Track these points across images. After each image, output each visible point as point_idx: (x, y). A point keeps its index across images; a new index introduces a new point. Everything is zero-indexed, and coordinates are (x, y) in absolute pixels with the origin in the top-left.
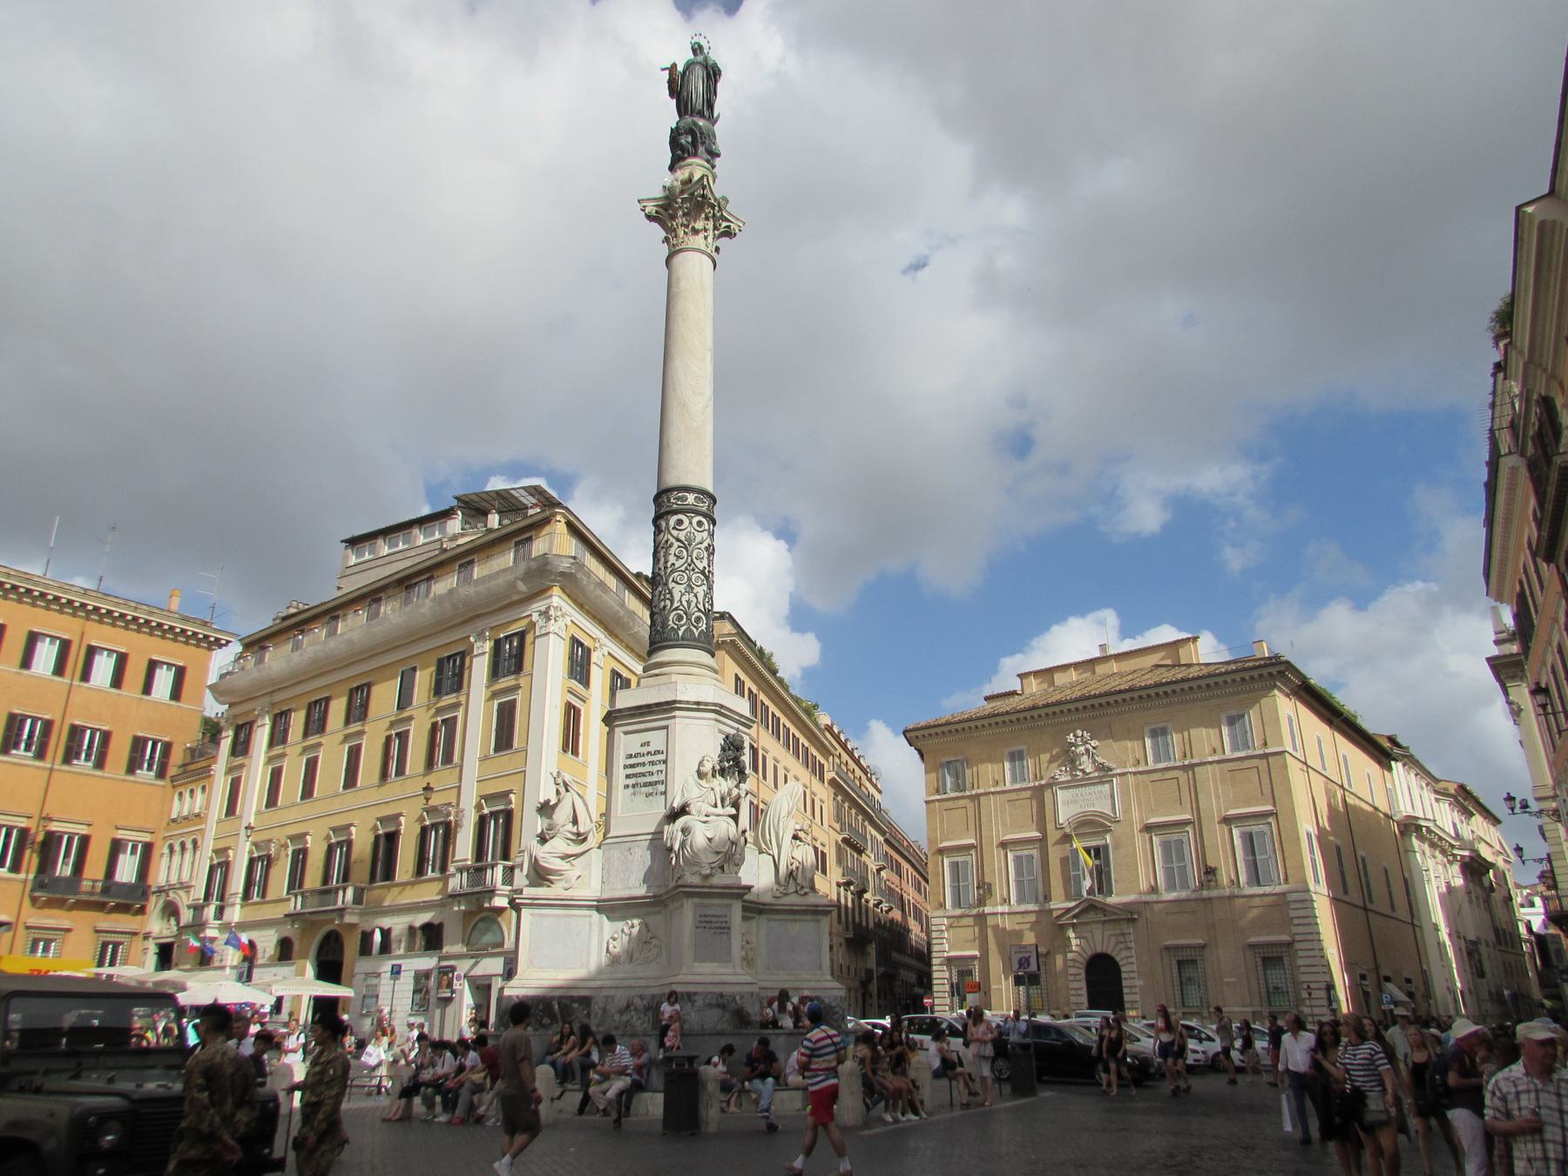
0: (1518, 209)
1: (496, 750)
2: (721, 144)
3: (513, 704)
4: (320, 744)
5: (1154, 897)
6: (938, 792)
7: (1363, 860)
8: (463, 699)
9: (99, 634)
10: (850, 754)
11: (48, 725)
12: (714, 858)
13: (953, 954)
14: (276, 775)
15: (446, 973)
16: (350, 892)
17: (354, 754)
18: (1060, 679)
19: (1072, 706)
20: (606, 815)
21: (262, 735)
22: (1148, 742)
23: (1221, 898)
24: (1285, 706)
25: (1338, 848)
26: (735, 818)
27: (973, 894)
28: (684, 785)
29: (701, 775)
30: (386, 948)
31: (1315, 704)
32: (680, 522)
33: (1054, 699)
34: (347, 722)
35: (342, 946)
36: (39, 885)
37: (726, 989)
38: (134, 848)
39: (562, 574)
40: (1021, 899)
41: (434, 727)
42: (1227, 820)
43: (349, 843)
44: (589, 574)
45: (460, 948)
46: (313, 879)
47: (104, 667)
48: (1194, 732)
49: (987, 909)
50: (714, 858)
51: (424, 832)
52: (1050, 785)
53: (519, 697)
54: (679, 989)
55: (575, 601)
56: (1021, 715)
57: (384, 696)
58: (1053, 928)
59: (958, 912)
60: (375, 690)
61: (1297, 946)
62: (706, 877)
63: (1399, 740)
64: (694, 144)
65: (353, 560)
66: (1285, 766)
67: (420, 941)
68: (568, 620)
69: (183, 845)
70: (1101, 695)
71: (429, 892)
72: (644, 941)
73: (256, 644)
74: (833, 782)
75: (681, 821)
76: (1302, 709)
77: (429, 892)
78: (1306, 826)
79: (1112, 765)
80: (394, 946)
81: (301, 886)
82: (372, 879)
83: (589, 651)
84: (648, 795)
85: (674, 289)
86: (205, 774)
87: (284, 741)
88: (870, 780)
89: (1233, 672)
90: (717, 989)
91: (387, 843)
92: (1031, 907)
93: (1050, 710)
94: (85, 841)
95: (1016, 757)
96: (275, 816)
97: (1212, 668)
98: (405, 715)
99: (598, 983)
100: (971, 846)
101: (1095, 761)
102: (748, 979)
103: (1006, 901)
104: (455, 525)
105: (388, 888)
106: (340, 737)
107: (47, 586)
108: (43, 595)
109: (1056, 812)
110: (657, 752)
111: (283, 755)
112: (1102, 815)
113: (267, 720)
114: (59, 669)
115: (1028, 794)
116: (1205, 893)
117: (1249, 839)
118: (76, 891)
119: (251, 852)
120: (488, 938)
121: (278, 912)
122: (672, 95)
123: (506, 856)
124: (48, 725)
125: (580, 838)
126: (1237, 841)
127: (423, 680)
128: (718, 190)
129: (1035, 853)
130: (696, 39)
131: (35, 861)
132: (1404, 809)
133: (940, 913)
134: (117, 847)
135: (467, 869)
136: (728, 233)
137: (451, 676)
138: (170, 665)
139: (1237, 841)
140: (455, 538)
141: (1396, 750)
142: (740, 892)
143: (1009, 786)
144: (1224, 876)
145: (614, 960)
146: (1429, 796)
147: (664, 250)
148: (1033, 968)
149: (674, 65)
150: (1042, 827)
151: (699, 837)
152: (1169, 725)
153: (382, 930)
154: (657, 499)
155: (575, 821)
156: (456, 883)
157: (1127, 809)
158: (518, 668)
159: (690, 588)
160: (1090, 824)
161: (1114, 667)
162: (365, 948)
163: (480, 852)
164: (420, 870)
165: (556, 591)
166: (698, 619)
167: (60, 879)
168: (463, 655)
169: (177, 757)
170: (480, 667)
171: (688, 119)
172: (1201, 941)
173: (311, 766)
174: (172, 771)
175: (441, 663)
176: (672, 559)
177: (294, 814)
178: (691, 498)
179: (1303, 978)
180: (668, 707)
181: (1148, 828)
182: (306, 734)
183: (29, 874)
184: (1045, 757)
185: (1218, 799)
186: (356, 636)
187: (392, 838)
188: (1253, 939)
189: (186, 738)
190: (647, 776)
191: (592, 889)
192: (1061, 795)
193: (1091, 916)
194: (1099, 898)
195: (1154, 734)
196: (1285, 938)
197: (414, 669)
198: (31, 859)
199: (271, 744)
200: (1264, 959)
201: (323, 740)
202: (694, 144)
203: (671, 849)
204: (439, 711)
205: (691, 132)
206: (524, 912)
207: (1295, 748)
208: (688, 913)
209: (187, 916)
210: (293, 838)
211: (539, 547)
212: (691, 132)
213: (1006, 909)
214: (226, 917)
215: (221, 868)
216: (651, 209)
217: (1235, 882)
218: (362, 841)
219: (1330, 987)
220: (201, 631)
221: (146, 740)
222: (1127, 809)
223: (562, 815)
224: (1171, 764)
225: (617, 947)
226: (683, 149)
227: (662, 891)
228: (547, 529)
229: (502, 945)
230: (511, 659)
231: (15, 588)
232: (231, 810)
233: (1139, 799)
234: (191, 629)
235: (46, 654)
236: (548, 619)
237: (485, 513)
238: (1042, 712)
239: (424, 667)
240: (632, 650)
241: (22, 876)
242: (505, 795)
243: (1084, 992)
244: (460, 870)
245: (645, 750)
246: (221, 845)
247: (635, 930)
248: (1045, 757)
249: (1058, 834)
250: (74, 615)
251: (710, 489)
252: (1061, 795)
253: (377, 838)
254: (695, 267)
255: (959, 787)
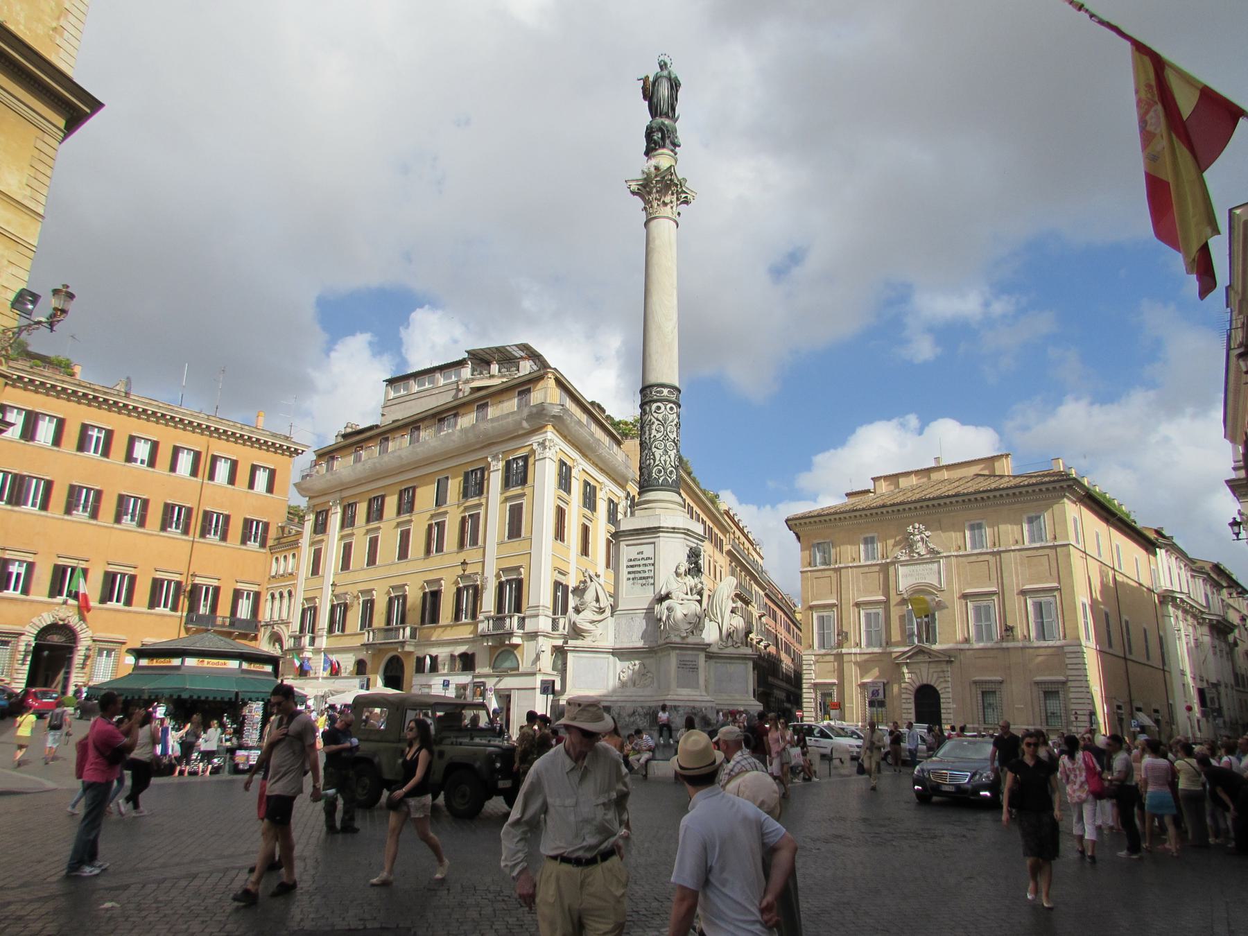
0: (1230, 211)
1: (509, 538)
2: (681, 136)
3: (520, 506)
4: (379, 528)
5: (966, 646)
6: (810, 565)
7: (1127, 622)
8: (483, 501)
9: (220, 447)
10: (741, 530)
11: (190, 510)
12: (688, 626)
13: (818, 681)
14: (347, 549)
15: (480, 688)
16: (408, 630)
17: (405, 536)
18: (903, 482)
19: (912, 506)
20: (615, 596)
21: (335, 520)
22: (968, 533)
23: (1015, 648)
24: (1072, 510)
25: (1107, 615)
26: (700, 602)
27: (834, 639)
28: (666, 579)
29: (678, 574)
30: (434, 668)
31: (1097, 508)
32: (659, 408)
33: (898, 500)
34: (399, 513)
35: (402, 666)
36: (189, 620)
37: (697, 705)
38: (248, 595)
39: (554, 417)
40: (869, 644)
41: (464, 520)
42: (1023, 593)
43: (405, 597)
44: (571, 415)
45: (487, 670)
46: (379, 620)
47: (223, 469)
48: (1002, 527)
49: (844, 651)
50: (688, 626)
51: (459, 592)
52: (893, 563)
53: (525, 501)
54: (668, 703)
55: (561, 434)
56: (874, 511)
57: (425, 496)
58: (894, 667)
59: (823, 651)
60: (418, 491)
61: (1070, 684)
62: (683, 638)
63: (1165, 533)
64: (663, 138)
65: (392, 395)
66: (1069, 555)
67: (458, 664)
68: (557, 448)
69: (281, 595)
70: (934, 499)
71: (464, 632)
72: (643, 673)
73: (327, 455)
74: (729, 553)
75: (666, 603)
76: (1085, 511)
77: (464, 632)
78: (1082, 598)
79: (940, 550)
80: (440, 667)
81: (370, 625)
82: (423, 622)
83: (595, 488)
84: (643, 585)
85: (651, 245)
86: (294, 545)
87: (352, 524)
88: (755, 550)
89: (1033, 485)
90: (692, 704)
91: (432, 599)
92: (877, 650)
93: (895, 508)
94: (217, 590)
95: (869, 541)
96: (347, 577)
97: (1018, 480)
98: (441, 510)
99: (614, 698)
100: (834, 605)
101: (927, 546)
102: (708, 698)
103: (858, 645)
104: (466, 372)
105: (435, 628)
106: (394, 523)
107: (184, 414)
108: (182, 420)
109: (897, 582)
110: (648, 558)
111: (352, 534)
112: (931, 586)
113: (339, 510)
114: (194, 472)
115: (877, 569)
116: (1005, 645)
117: (1039, 607)
118: (214, 624)
119: (332, 601)
120: (507, 664)
121: (357, 642)
122: (645, 97)
123: (518, 609)
124: (190, 510)
125: (601, 611)
126: (1030, 608)
127: (454, 486)
128: (680, 173)
129: (881, 611)
130: (662, 58)
131: (187, 603)
132: (1164, 584)
133: (809, 652)
134: (237, 594)
135: (492, 618)
136: (686, 202)
137: (475, 485)
138: (265, 468)
139: (1030, 608)
140: (467, 381)
141: (1161, 540)
142: (704, 648)
143: (863, 562)
144: (1019, 632)
145: (624, 685)
146: (1185, 574)
147: (643, 217)
148: (881, 696)
149: (647, 77)
150: (886, 593)
151: (679, 613)
152: (984, 522)
153: (431, 657)
154: (641, 391)
155: (597, 600)
156: (483, 627)
157: (949, 582)
158: (524, 481)
159: (666, 452)
160: (920, 591)
161: (946, 475)
162: (420, 668)
163: (500, 606)
164: (457, 617)
165: (550, 428)
166: (671, 472)
167: (204, 616)
168: (483, 470)
169: (273, 533)
170: (495, 480)
171: (659, 120)
172: (999, 678)
173: (374, 543)
174: (270, 542)
175: (466, 476)
176: (654, 432)
177: (362, 576)
178: (665, 391)
179: (1073, 707)
180: (655, 530)
181: (965, 596)
182: (368, 520)
183: (183, 613)
184: (891, 542)
185: (1017, 576)
186: (404, 453)
187: (436, 595)
188: (1038, 678)
189: (277, 520)
190: (643, 573)
191: (609, 642)
192: (902, 570)
193: (920, 658)
194: (926, 645)
195: (972, 528)
196: (1062, 678)
197: (447, 478)
198: (184, 602)
199: (343, 526)
200: (1045, 693)
201: (381, 525)
202: (663, 138)
203: (660, 620)
204: (466, 509)
205: (660, 129)
206: (570, 655)
207: (1077, 541)
208: (673, 658)
209: (289, 643)
210: (362, 592)
211: (536, 397)
212: (660, 129)
213: (858, 650)
214: (317, 644)
215: (310, 612)
216: (634, 187)
217: (1027, 638)
218: (414, 595)
219: (1092, 714)
220: (286, 444)
221: (252, 521)
222: (949, 582)
223: (589, 596)
224: (984, 550)
225: (625, 677)
226: (656, 143)
227: (654, 644)
228: (541, 385)
229: (518, 669)
230: (518, 475)
231: (164, 415)
232: (315, 570)
233: (959, 574)
234: (278, 443)
235: (185, 461)
236: (545, 448)
237: (488, 363)
238: (890, 509)
239: (455, 477)
240: (597, 465)
241: (179, 613)
242: (517, 569)
243: (913, 711)
244: (488, 619)
245: (640, 556)
246: (310, 595)
247: (637, 667)
248: (891, 542)
249: (898, 599)
250: (202, 434)
251: (677, 385)
252: (902, 570)
253: (425, 594)
254: (664, 229)
255: (825, 562)
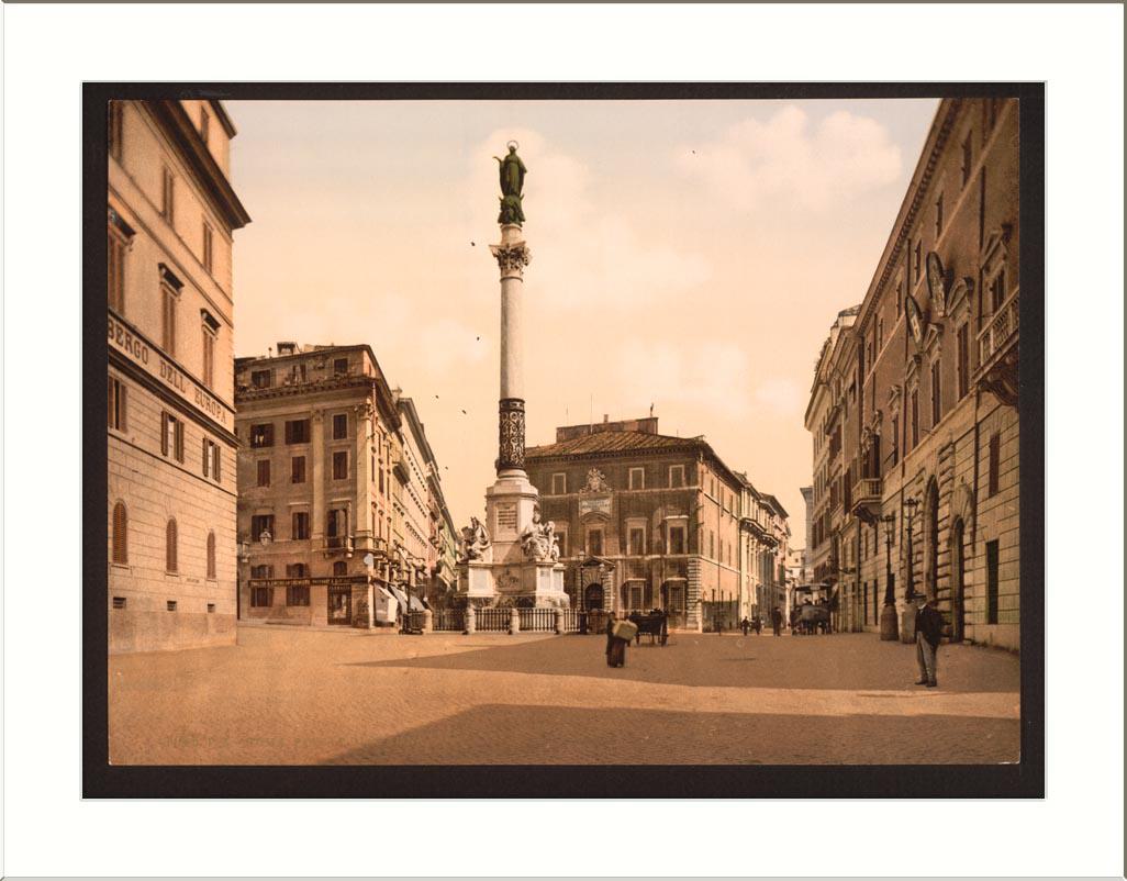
75: (529, 539)
154: (500, 402)
176: (512, 431)
178: (518, 404)
202: (515, 215)
223: (478, 534)
226: (510, 218)
